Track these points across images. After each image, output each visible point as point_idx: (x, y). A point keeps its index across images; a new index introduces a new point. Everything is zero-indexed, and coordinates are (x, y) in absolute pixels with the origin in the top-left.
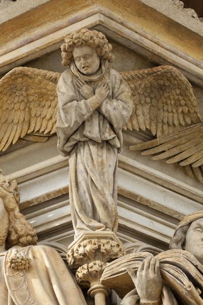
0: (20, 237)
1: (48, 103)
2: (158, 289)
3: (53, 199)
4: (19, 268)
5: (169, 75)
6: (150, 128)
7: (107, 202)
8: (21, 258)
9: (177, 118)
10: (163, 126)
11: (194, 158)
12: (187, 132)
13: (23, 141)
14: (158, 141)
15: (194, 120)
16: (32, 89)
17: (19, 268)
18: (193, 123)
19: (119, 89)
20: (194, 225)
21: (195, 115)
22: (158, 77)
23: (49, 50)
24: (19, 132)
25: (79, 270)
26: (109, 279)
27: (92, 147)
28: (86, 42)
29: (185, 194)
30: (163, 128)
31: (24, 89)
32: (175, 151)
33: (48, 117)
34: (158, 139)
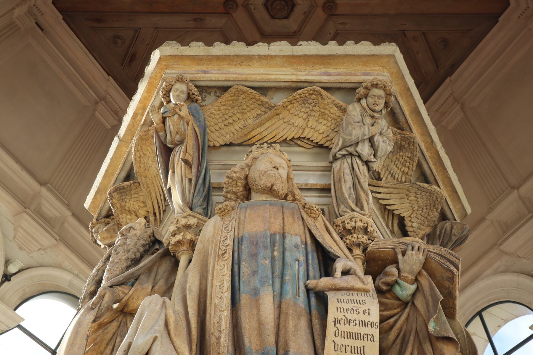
1: (326, 122)
2: (420, 269)
5: (412, 140)
9: (398, 174)
12: (401, 187)
14: (382, 183)
15: (407, 180)
16: (319, 107)
18: (405, 181)
19: (386, 131)
21: (409, 177)
22: (404, 139)
23: (343, 85)
24: (294, 133)
25: (348, 237)
27: (358, 161)
28: (385, 86)
31: (313, 104)
32: (387, 196)
33: (321, 131)
34: (382, 182)
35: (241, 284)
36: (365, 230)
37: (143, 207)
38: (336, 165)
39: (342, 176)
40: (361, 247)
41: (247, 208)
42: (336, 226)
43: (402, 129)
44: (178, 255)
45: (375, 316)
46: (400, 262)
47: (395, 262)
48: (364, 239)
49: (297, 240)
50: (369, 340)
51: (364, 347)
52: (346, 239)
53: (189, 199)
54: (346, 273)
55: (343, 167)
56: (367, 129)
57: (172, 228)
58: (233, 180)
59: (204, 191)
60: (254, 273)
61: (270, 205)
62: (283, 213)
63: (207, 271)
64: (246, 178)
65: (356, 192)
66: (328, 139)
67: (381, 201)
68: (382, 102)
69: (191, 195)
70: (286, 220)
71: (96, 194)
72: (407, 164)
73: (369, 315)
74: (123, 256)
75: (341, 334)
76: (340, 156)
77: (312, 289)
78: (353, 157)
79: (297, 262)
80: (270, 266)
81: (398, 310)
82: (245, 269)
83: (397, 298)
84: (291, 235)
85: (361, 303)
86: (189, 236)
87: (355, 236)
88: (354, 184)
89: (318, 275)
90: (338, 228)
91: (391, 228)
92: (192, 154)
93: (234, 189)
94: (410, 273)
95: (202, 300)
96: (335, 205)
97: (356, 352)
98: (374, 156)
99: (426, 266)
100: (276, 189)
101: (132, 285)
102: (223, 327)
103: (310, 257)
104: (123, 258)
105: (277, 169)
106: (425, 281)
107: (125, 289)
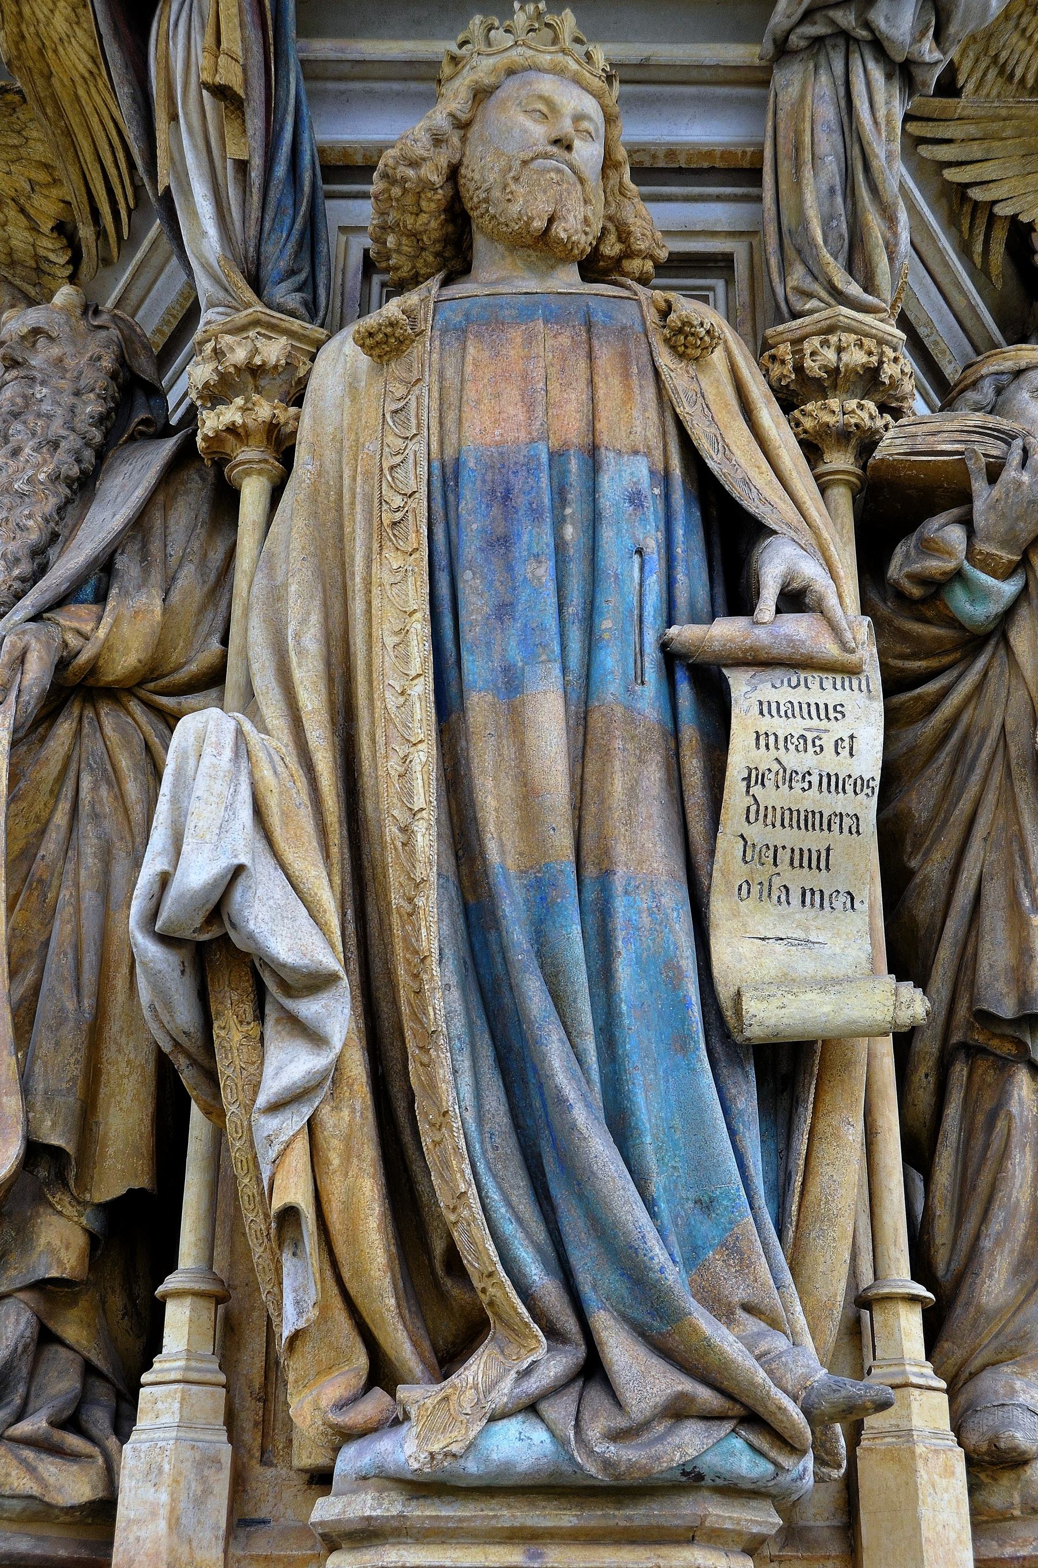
0: (629, 254)
3: (712, 169)
4: (689, 351)
6: (960, 62)
7: (896, 245)
8: (707, 326)
10: (988, 68)
11: (1006, 188)
14: (962, 105)
17: (689, 351)
25: (809, 407)
26: (898, 460)
27: (871, 65)
29: (940, 278)
30: (985, 74)
32: (976, 151)
35: (464, 654)
36: (870, 381)
37: (47, 185)
38: (789, 82)
39: (807, 139)
40: (853, 442)
41: (464, 331)
42: (773, 358)
44: (232, 473)
45: (868, 761)
46: (979, 505)
47: (966, 498)
48: (864, 412)
50: (846, 830)
51: (828, 850)
52: (804, 413)
53: (245, 241)
54: (794, 599)
55: (808, 93)
57: (200, 373)
58: (405, 191)
59: (296, 205)
60: (504, 610)
61: (546, 321)
62: (590, 356)
63: (343, 566)
64: (454, 173)
65: (854, 204)
69: (253, 231)
70: (601, 393)
73: (851, 755)
74: (38, 467)
75: (766, 816)
76: (803, 44)
78: (853, 47)
79: (636, 558)
80: (551, 586)
81: (957, 655)
82: (476, 605)
83: (953, 622)
84: (619, 453)
85: (832, 715)
86: (264, 411)
87: (834, 403)
90: (776, 370)
91: (978, 260)
92: (238, 50)
93: (410, 220)
94: (1004, 544)
95: (338, 673)
96: (773, 261)
97: (805, 863)
98: (938, 37)
100: (563, 235)
101: (101, 598)
102: (419, 802)
103: (679, 532)
104: (42, 477)
105: (569, 148)
107: (80, 619)
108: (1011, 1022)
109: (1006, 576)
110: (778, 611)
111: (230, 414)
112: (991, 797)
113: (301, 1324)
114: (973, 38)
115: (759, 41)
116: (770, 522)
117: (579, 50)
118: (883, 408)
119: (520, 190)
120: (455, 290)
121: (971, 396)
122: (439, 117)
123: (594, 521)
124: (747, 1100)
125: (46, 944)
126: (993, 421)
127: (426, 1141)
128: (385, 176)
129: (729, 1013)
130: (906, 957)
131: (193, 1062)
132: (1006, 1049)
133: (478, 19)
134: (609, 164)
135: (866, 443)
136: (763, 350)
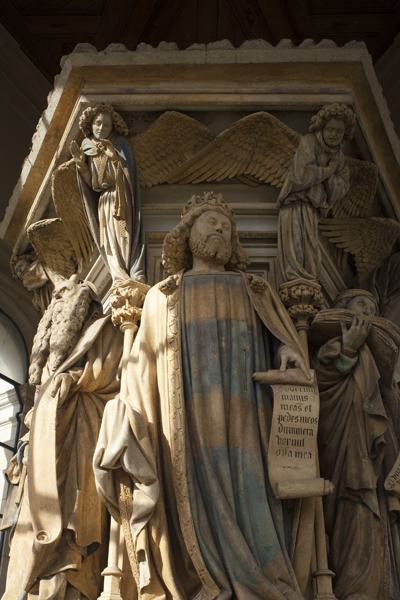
0: (239, 263)
1: (272, 155)
13: (236, 180)
14: (333, 221)
18: (360, 217)
20: (358, 299)
24: (238, 168)
33: (268, 167)
38: (285, 214)
43: (360, 157)
46: (344, 336)
48: (309, 309)
49: (243, 326)
54: (291, 364)
56: (320, 171)
66: (277, 176)
67: (331, 240)
68: (341, 136)
71: (11, 224)
72: (364, 198)
77: (258, 381)
83: (338, 371)
87: (301, 306)
88: (302, 239)
89: (264, 367)
90: (284, 296)
94: (352, 348)
99: (369, 340)
101: (83, 366)
106: (366, 356)
108: (358, 491)
109: (352, 357)
110: (287, 368)
111: (121, 311)
112: (349, 423)
113: (146, 585)
114: (337, 202)
115: (275, 202)
116: (283, 341)
117: (224, 205)
118: (315, 307)
119: (207, 245)
120: (188, 273)
121: (340, 304)
122: (182, 224)
123: (229, 343)
124: (280, 517)
125: (68, 469)
126: (348, 311)
127: (183, 530)
128: (167, 241)
129: (274, 490)
130: (325, 472)
131: (112, 505)
132: (356, 499)
133: (194, 197)
134: (233, 237)
135: (310, 318)
136: (280, 290)
